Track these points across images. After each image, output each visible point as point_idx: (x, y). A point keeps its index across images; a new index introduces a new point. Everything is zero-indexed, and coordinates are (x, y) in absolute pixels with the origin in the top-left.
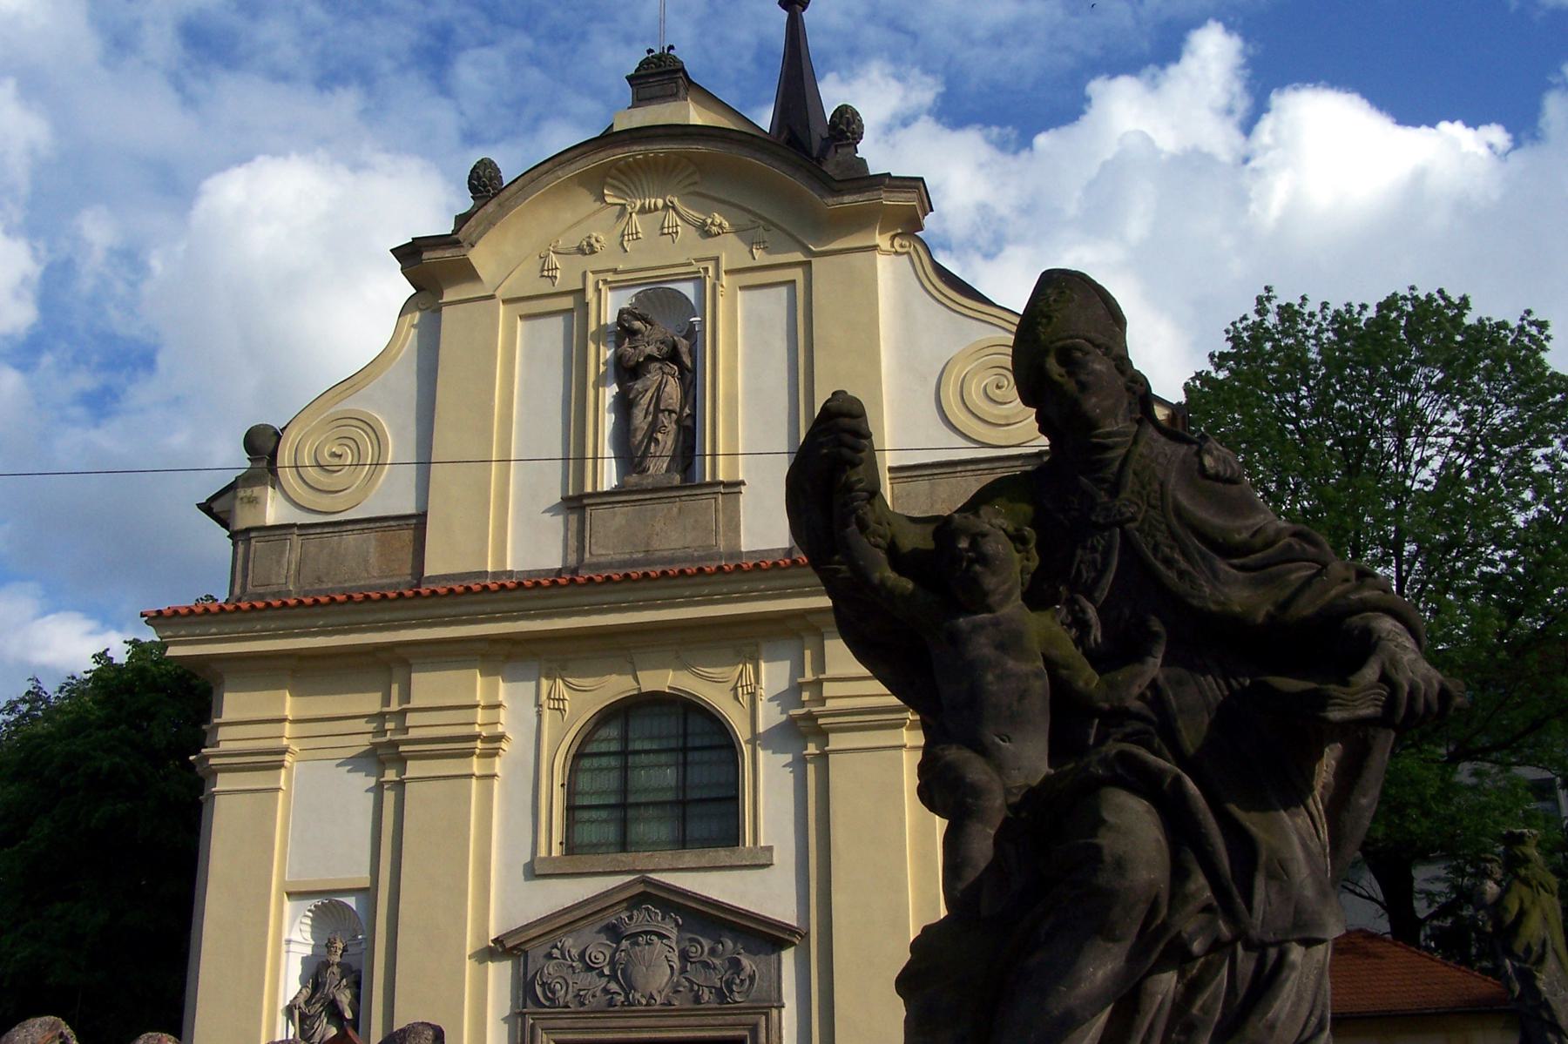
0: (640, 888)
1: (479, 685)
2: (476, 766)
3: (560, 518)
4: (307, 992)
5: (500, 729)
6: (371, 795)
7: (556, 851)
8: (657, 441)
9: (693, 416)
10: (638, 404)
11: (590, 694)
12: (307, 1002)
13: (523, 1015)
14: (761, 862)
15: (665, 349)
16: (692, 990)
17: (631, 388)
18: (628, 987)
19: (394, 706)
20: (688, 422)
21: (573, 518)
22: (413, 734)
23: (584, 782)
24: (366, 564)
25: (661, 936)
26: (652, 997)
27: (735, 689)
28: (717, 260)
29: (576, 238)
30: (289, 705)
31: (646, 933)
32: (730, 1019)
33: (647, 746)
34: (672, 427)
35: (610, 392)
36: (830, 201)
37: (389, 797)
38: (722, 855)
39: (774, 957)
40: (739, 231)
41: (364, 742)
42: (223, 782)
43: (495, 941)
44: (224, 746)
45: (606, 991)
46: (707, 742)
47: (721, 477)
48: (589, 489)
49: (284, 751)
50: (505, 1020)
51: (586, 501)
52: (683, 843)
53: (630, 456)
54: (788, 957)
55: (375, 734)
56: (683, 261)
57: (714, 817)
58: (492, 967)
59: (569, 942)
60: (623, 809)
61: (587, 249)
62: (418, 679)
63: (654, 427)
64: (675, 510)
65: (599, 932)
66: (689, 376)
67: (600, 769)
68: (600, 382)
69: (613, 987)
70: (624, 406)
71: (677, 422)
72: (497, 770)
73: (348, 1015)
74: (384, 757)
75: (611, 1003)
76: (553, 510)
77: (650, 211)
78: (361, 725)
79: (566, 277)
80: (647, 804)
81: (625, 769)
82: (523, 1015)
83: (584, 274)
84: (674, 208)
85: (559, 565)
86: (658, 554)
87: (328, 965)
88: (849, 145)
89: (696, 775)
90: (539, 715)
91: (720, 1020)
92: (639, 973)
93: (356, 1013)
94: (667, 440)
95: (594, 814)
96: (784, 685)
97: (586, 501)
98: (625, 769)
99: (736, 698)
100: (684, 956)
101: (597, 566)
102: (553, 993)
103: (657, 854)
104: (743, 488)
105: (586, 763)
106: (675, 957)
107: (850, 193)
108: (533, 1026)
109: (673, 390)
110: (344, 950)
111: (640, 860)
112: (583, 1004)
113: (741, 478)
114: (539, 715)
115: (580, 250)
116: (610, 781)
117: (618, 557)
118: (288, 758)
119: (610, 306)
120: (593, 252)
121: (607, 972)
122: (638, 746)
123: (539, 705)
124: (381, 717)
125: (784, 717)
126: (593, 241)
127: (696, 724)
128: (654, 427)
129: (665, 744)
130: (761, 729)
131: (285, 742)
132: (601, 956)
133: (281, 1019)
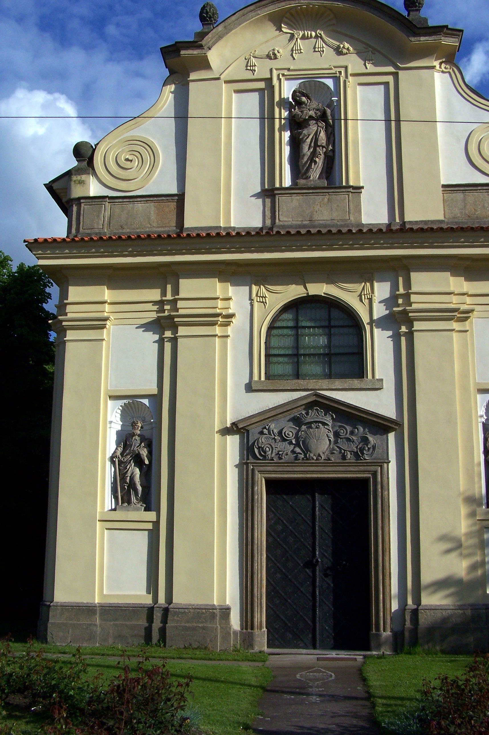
0: (314, 398)
1: (218, 288)
2: (218, 330)
3: (260, 201)
4: (120, 450)
5: (231, 311)
6: (156, 345)
7: (263, 378)
8: (315, 162)
9: (333, 151)
10: (305, 141)
12: (122, 454)
13: (247, 464)
15: (319, 114)
16: (340, 452)
17: (300, 134)
18: (306, 449)
19: (169, 297)
20: (331, 154)
21: (268, 201)
22: (181, 312)
23: (274, 342)
24: (152, 220)
25: (324, 424)
26: (319, 455)
27: (360, 296)
28: (346, 68)
29: (266, 50)
30: (107, 294)
31: (316, 422)
32: (362, 468)
33: (309, 324)
34: (322, 156)
35: (287, 135)
36: (413, 39)
37: (168, 346)
38: (356, 383)
39: (385, 436)
40: (359, 53)
41: (154, 315)
42: (70, 335)
43: (233, 424)
44: (70, 316)
45: (293, 452)
46: (341, 323)
47: (351, 183)
48: (277, 185)
49: (106, 319)
50: (236, 466)
51: (276, 192)
52: (330, 376)
54: (391, 436)
55: (157, 312)
56: (327, 67)
57: (352, 363)
58: (229, 438)
59: (272, 426)
60: (296, 356)
61: (272, 56)
62: (183, 282)
63: (314, 154)
64: (326, 200)
65: (288, 421)
66: (330, 130)
67: (284, 336)
68: (282, 129)
69: (298, 450)
70: (296, 144)
71: (325, 153)
72: (229, 333)
73: (147, 462)
74: (165, 325)
75: (296, 458)
76: (257, 196)
77: (308, 38)
78: (150, 306)
79: (262, 70)
80: (309, 355)
81: (297, 337)
82: (247, 464)
83: (271, 70)
84: (321, 38)
85: (260, 226)
86: (316, 223)
87: (134, 435)
88: (417, 10)
89: (336, 341)
90: (252, 306)
91: (356, 469)
92: (313, 443)
93: (150, 462)
94: (320, 161)
95: (281, 359)
96: (387, 295)
97: (276, 192)
98: (297, 337)
99: (361, 300)
100: (337, 435)
101: (283, 227)
102: (265, 452)
103: (320, 381)
104: (363, 190)
105: (275, 332)
106: (331, 435)
107: (425, 35)
108: (253, 470)
109: (322, 135)
110: (142, 427)
111: (312, 384)
112: (280, 458)
113: (361, 185)
114: (252, 306)
115: (268, 57)
116: (289, 342)
117: (294, 223)
118: (108, 323)
119: (287, 90)
120: (276, 58)
121: (294, 442)
122: (304, 324)
123: (251, 299)
124: (161, 303)
125: (387, 312)
126: (276, 52)
127: (335, 313)
128: (314, 154)
129: (318, 324)
130: (375, 317)
131: (106, 314)
132: (291, 433)
133: (108, 463)
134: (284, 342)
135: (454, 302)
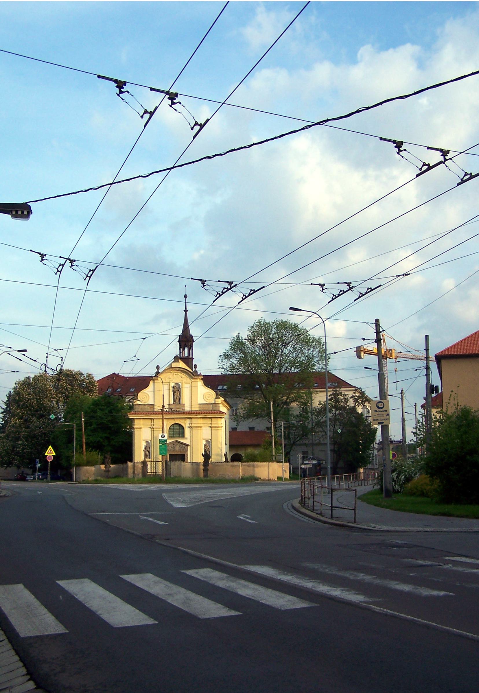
14: (186, 439)
24: (148, 409)
53: (174, 401)
54: (189, 447)
94: (178, 399)
119: (173, 384)
134: (172, 431)
135: (199, 425)
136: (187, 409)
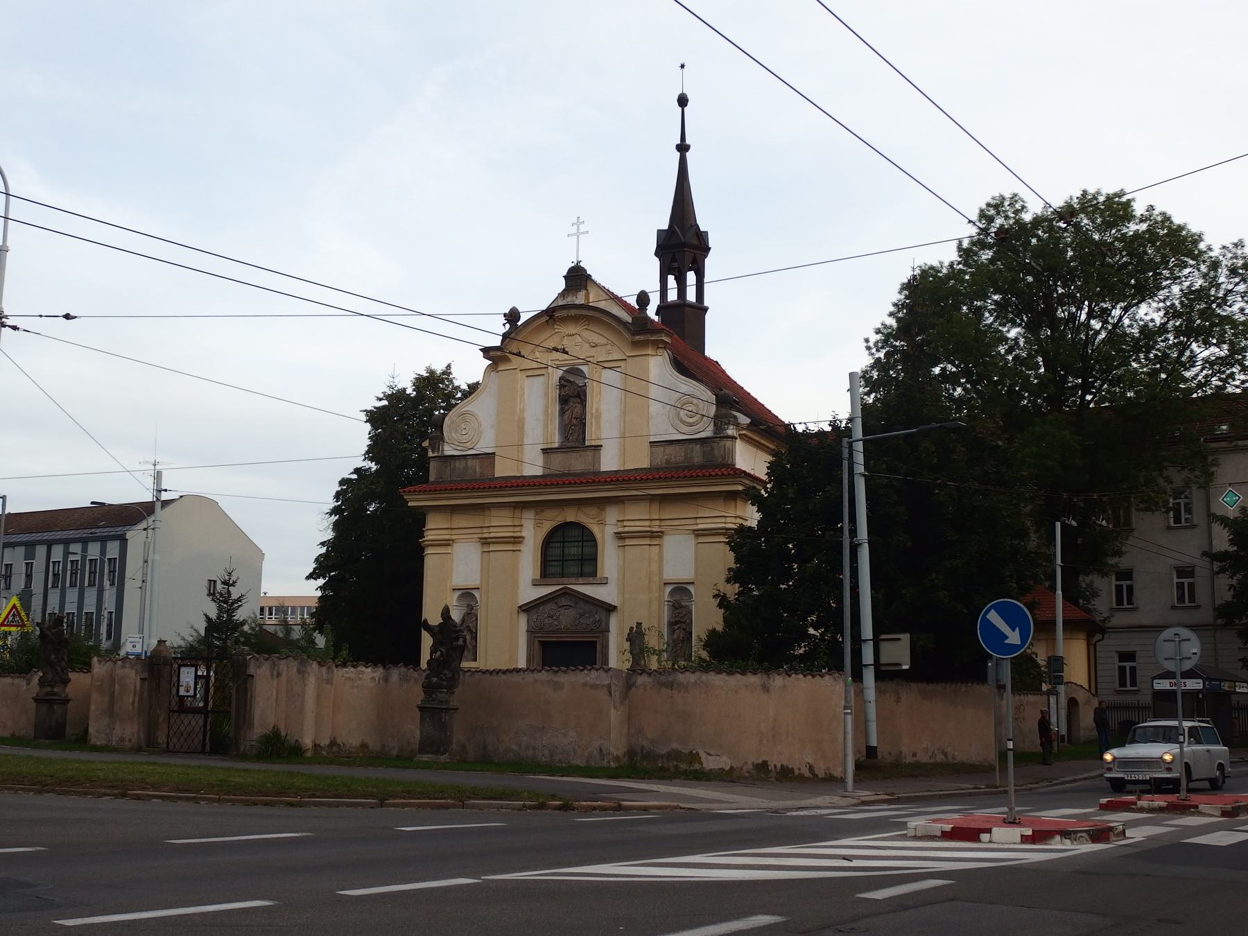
11: (552, 519)
14: (604, 582)
42: (428, 551)
52: (581, 575)
57: (588, 565)
111: (566, 580)
136: (609, 462)
